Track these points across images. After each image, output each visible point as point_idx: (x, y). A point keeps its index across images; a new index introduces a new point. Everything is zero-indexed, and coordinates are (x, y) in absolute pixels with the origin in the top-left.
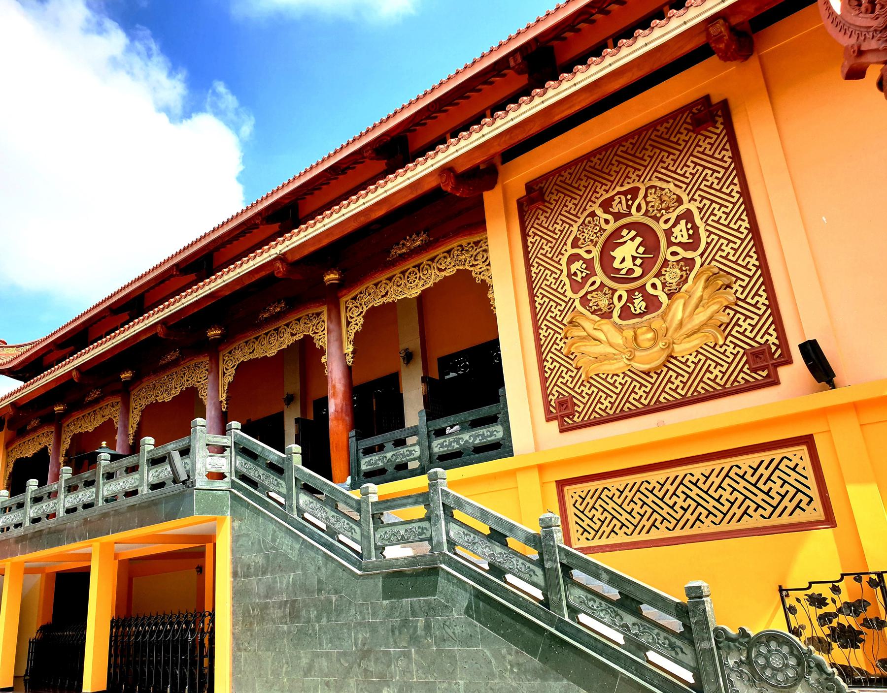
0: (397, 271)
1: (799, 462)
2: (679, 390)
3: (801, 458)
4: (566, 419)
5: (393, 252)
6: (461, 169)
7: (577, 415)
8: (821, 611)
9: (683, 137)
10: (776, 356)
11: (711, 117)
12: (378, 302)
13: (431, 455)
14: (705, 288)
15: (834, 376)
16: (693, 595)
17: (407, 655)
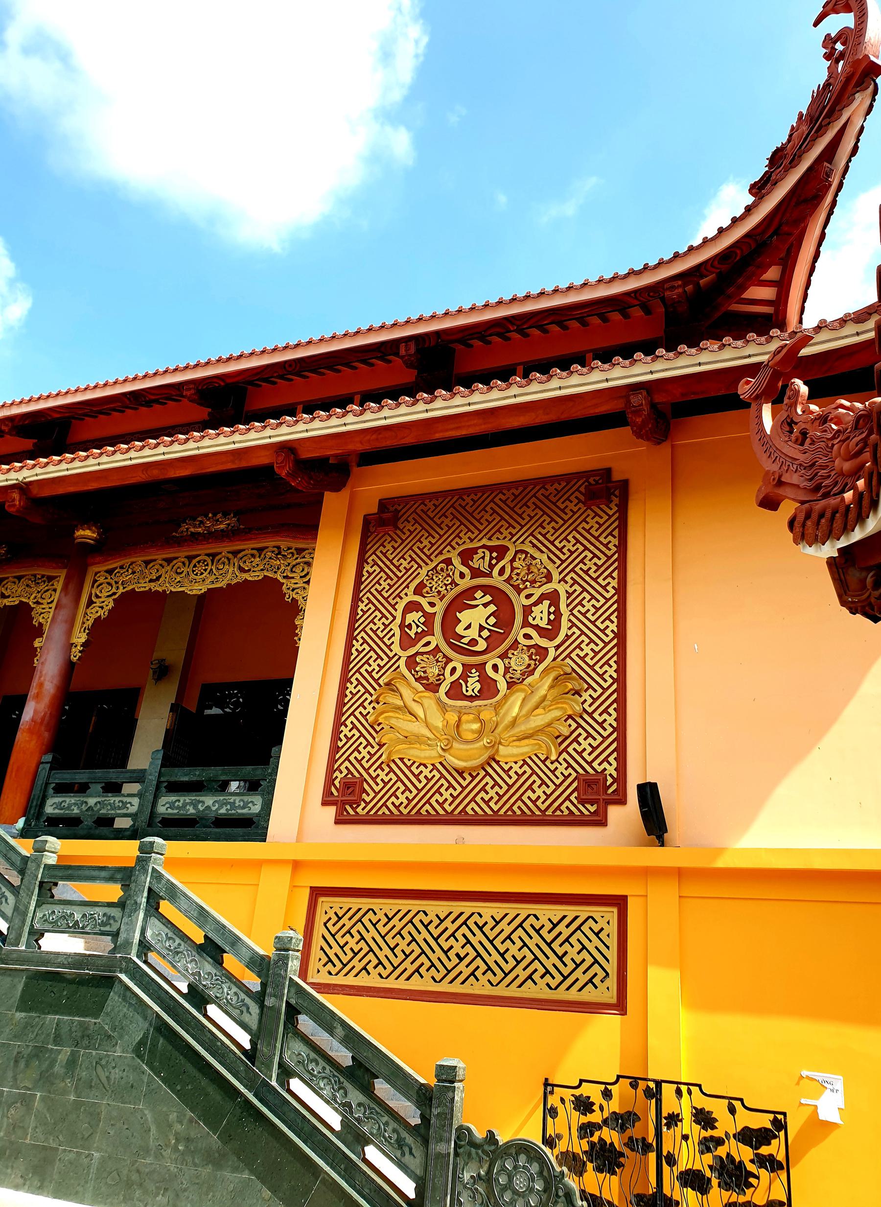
0: (182, 554)
1: (605, 926)
2: (492, 804)
3: (608, 923)
4: (348, 807)
5: (184, 527)
6: (305, 455)
7: (363, 805)
8: (584, 1119)
9: (571, 506)
10: (610, 790)
11: (606, 495)
12: (143, 586)
13: (153, 814)
14: (551, 687)
15: (666, 831)
16: (444, 1077)
17: (26, 1101)
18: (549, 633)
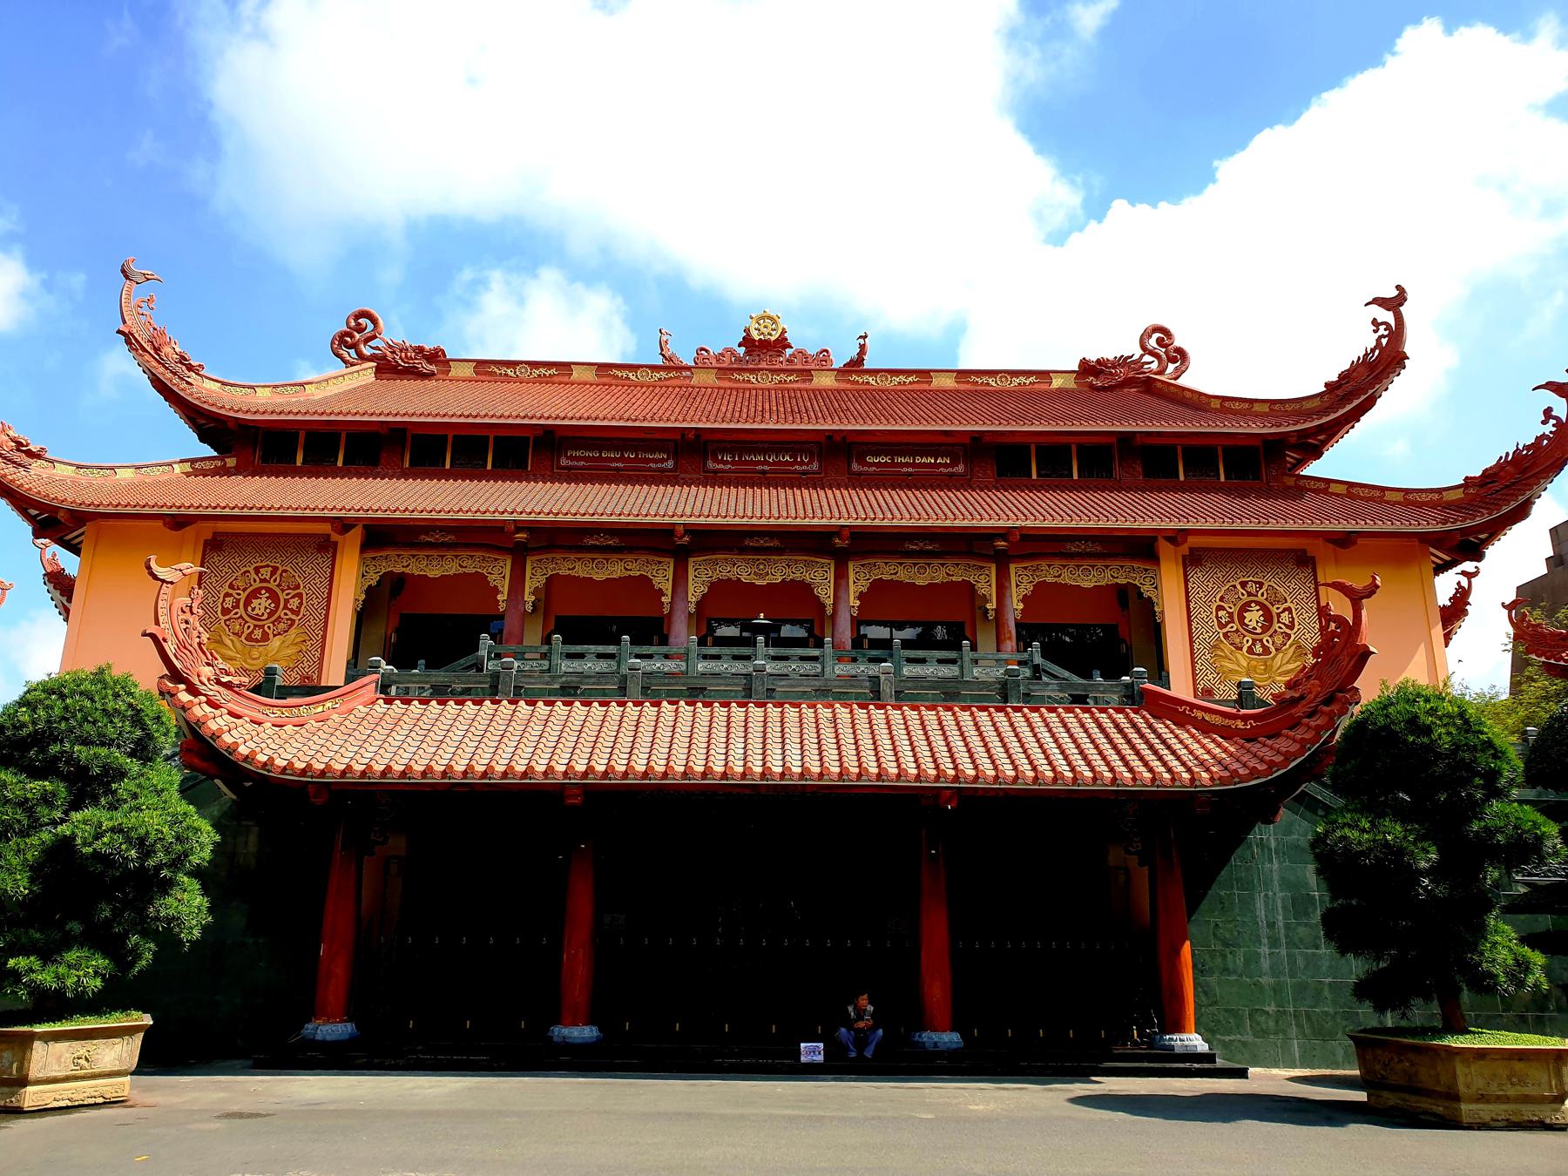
12: (1050, 579)
18: (1291, 627)
